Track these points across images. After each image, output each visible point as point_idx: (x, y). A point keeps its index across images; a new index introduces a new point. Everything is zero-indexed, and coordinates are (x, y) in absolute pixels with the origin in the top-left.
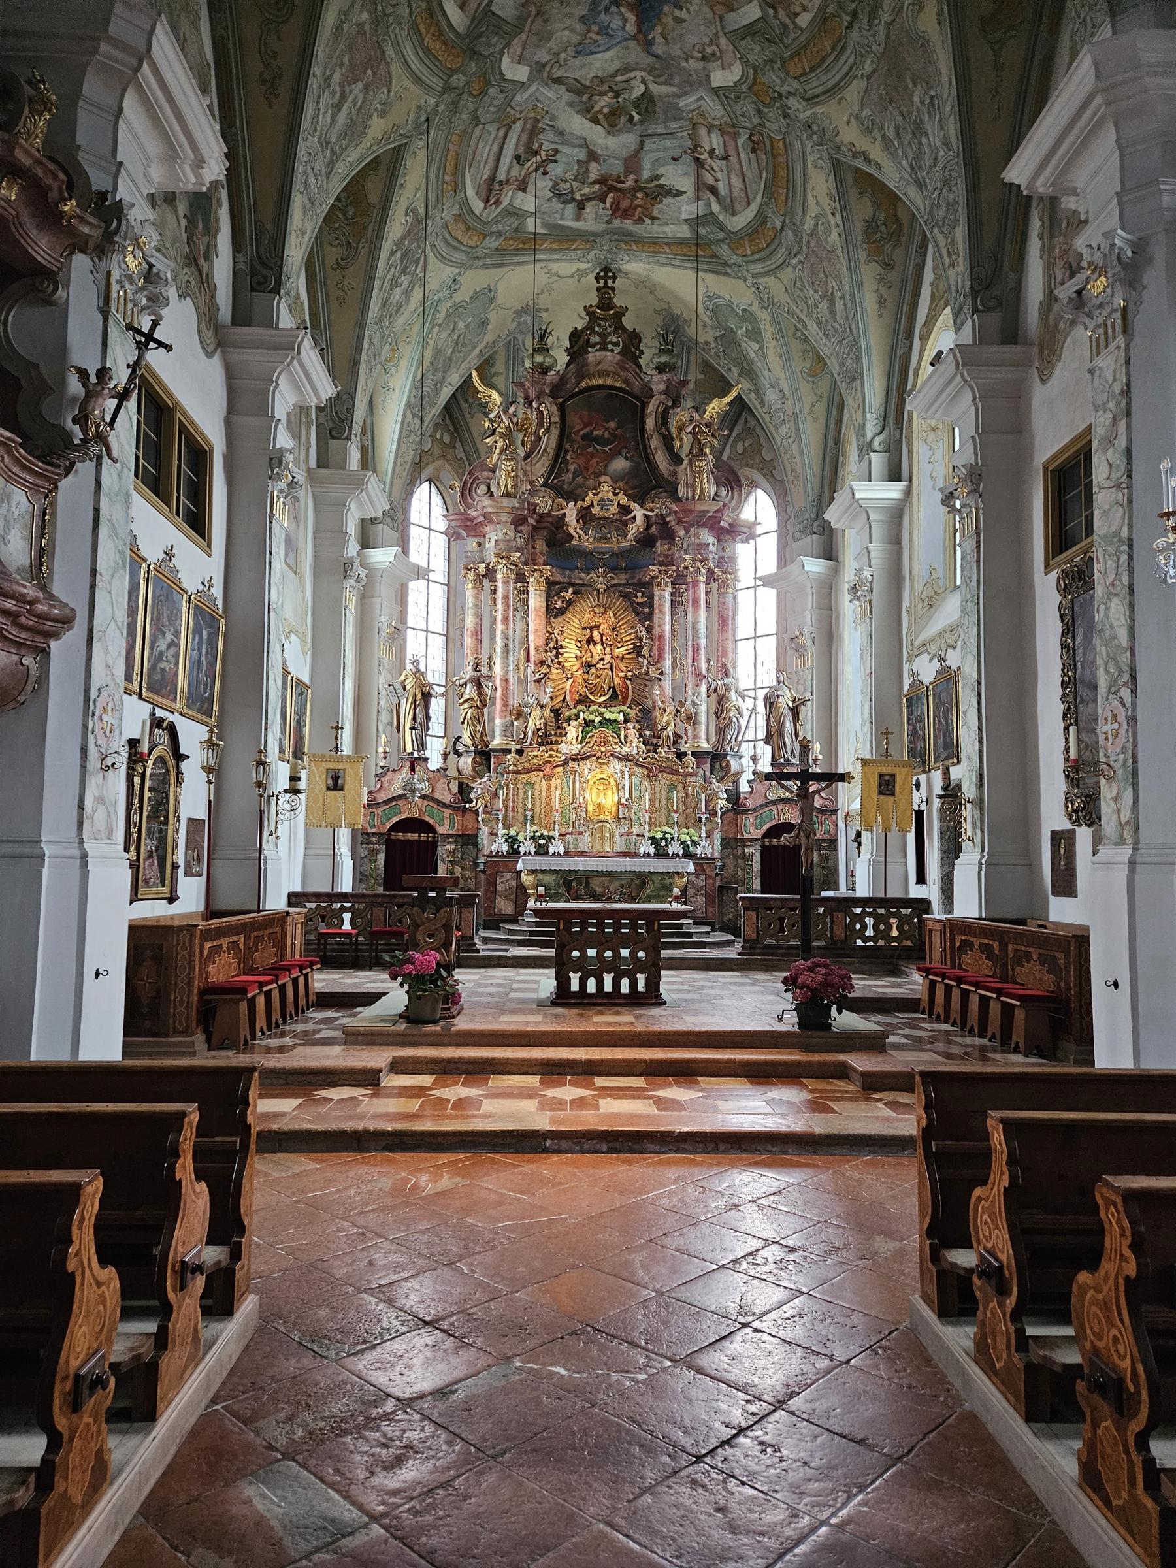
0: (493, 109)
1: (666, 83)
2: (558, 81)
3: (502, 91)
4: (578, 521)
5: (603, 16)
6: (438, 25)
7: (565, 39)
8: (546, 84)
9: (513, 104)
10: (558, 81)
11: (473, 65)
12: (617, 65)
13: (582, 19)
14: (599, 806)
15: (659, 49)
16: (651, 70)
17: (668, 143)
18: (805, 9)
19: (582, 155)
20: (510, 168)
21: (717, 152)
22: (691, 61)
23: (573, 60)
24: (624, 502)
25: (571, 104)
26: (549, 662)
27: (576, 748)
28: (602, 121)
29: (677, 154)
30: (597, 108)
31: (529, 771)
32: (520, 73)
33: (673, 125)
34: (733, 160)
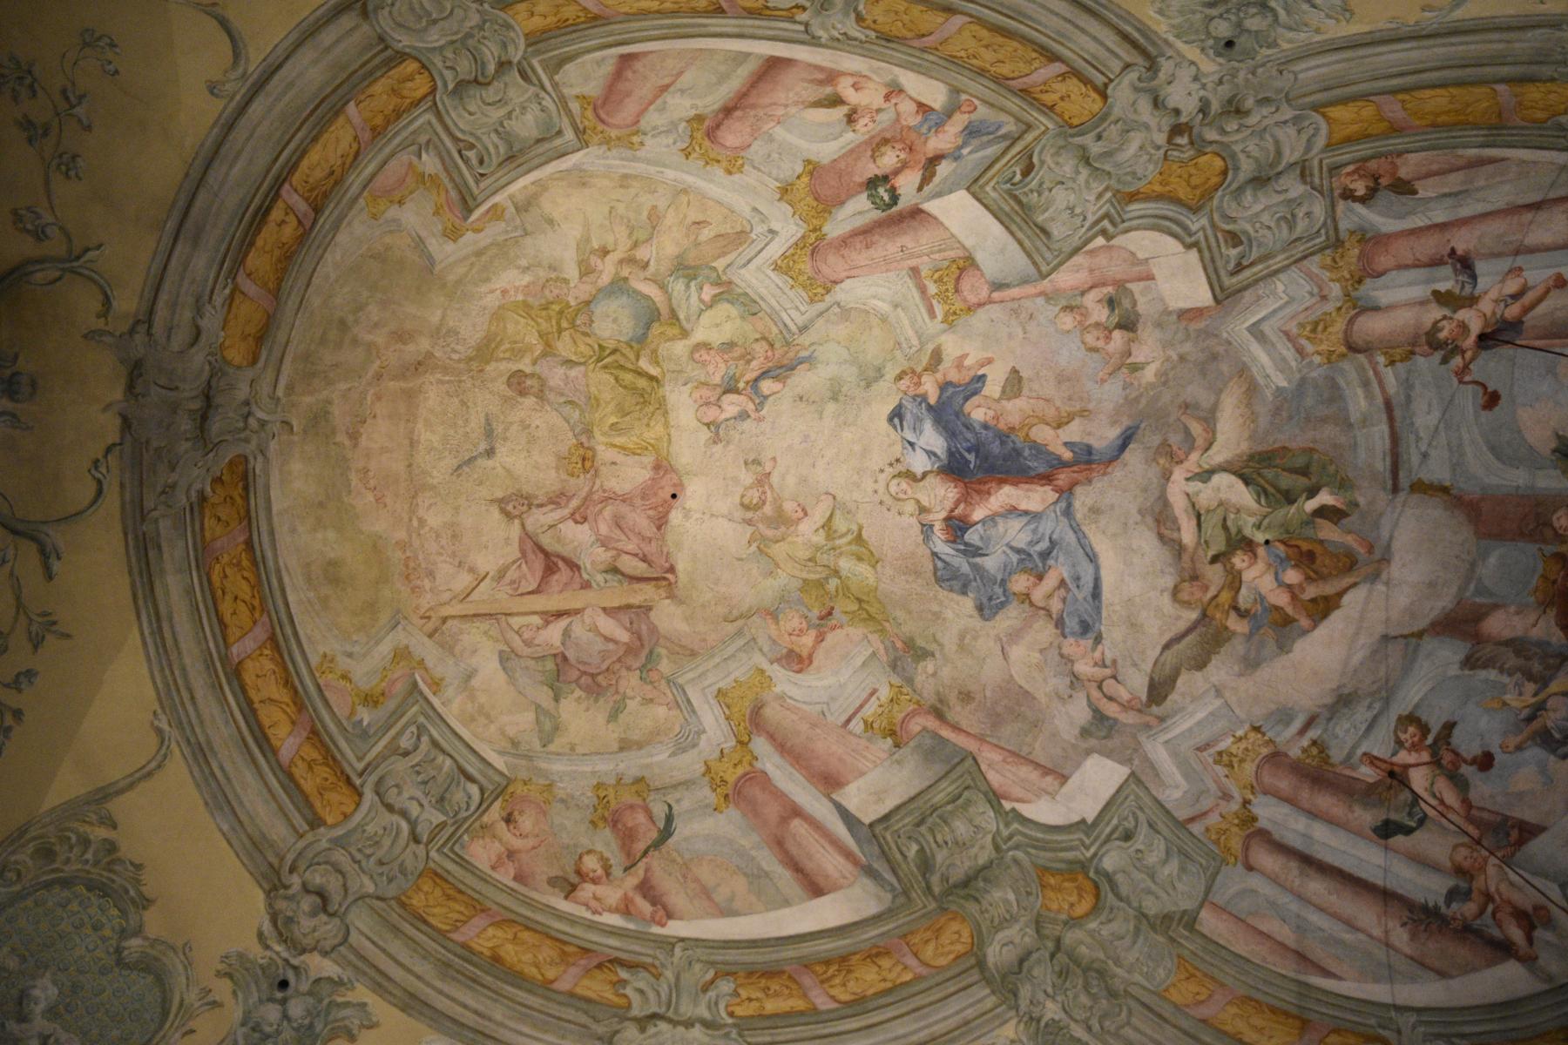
0: (1173, 867)
1: (1209, 420)
2: (1159, 690)
3: (1128, 836)
5: (991, 563)
6: (807, 965)
7: (1036, 657)
8: (1162, 719)
9: (1182, 814)
10: (1159, 690)
11: (997, 894)
12: (1146, 542)
13: (986, 610)
15: (1104, 435)
16: (1169, 455)
17: (1425, 417)
18: (894, 91)
19: (1446, 655)
20: (1420, 861)
21: (1443, 287)
22: (1139, 356)
23: (1106, 642)
25: (1251, 664)
28: (1329, 589)
29: (1468, 399)
30: (1281, 599)
32: (1097, 780)
33: (1358, 402)
34: (1462, 241)
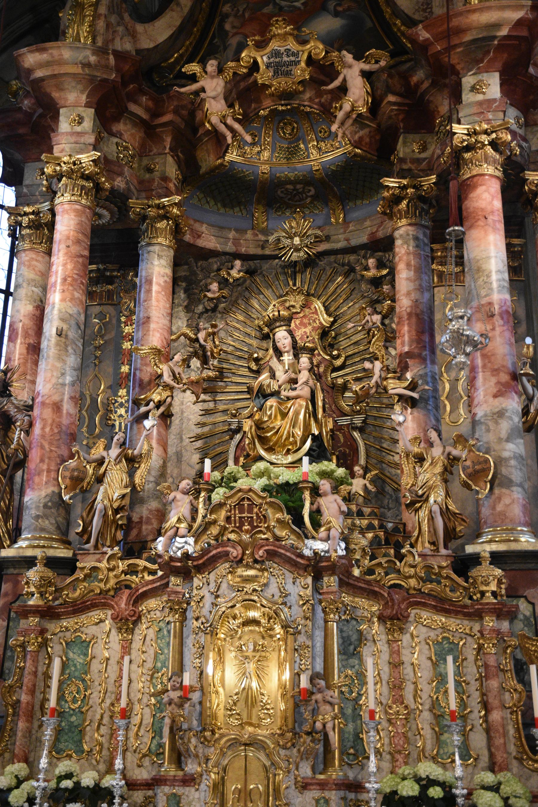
4: (231, 106)
14: (249, 699)
24: (317, 48)
26: (167, 378)
27: (185, 545)
31: (80, 608)
